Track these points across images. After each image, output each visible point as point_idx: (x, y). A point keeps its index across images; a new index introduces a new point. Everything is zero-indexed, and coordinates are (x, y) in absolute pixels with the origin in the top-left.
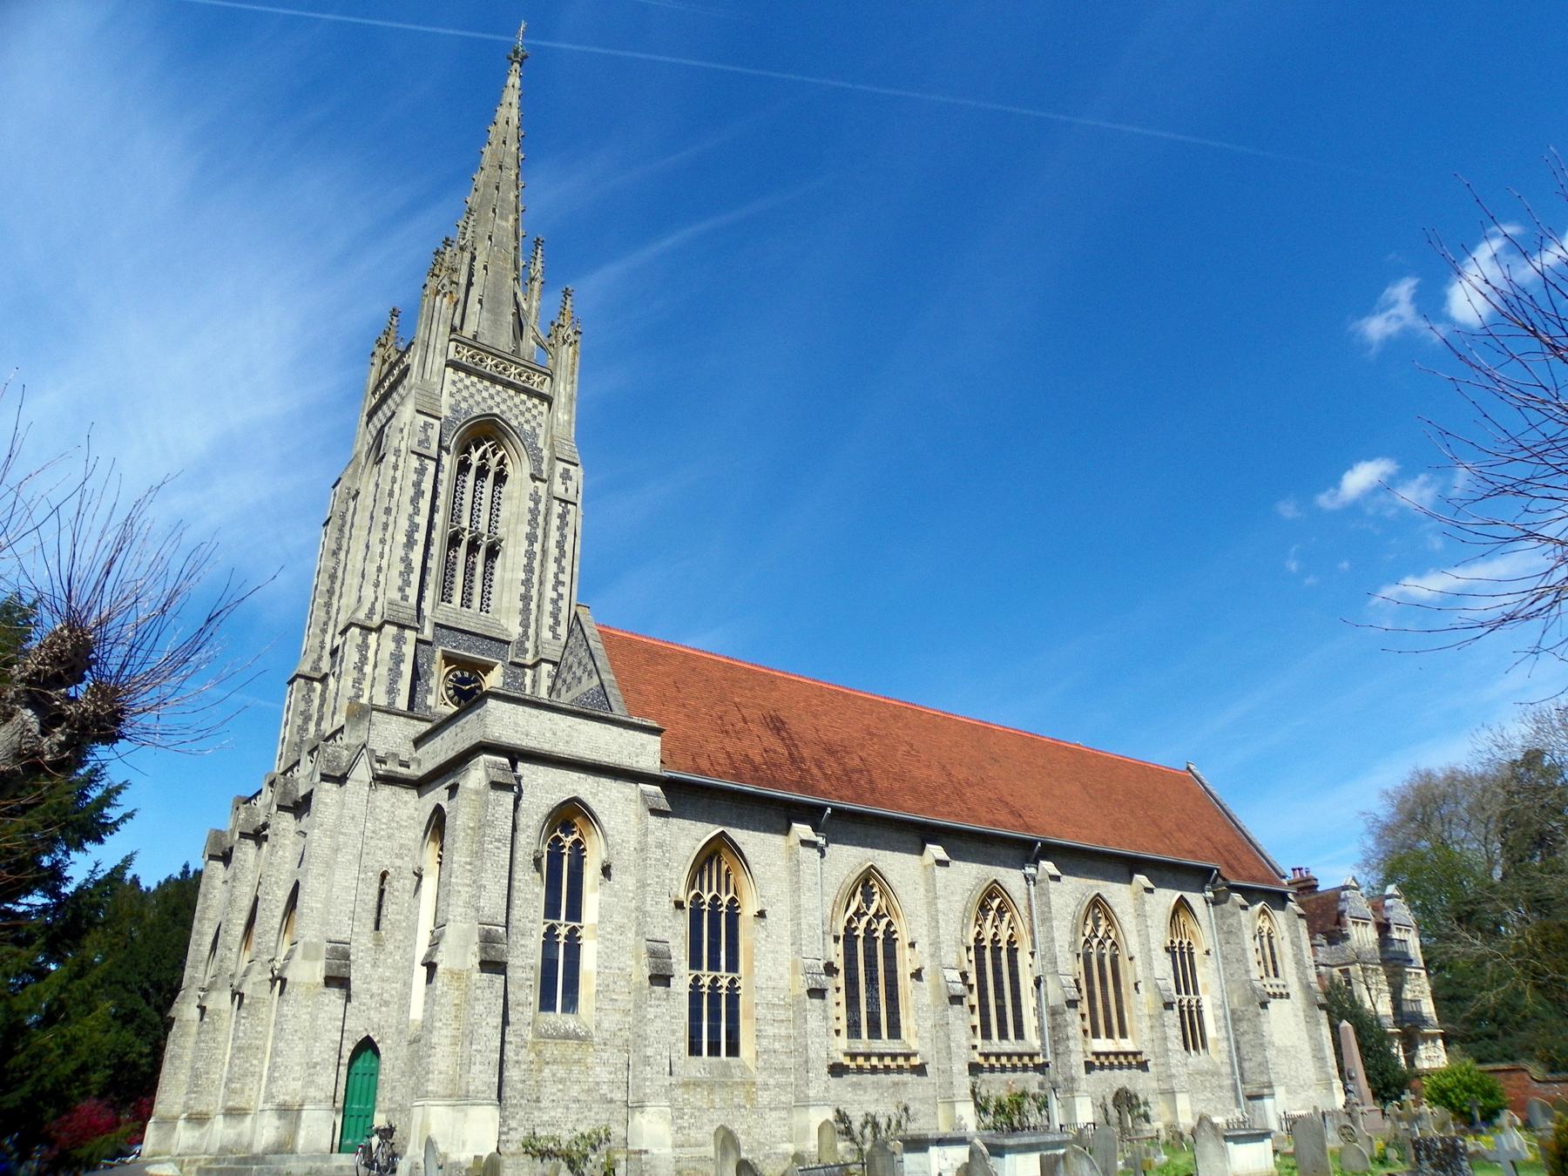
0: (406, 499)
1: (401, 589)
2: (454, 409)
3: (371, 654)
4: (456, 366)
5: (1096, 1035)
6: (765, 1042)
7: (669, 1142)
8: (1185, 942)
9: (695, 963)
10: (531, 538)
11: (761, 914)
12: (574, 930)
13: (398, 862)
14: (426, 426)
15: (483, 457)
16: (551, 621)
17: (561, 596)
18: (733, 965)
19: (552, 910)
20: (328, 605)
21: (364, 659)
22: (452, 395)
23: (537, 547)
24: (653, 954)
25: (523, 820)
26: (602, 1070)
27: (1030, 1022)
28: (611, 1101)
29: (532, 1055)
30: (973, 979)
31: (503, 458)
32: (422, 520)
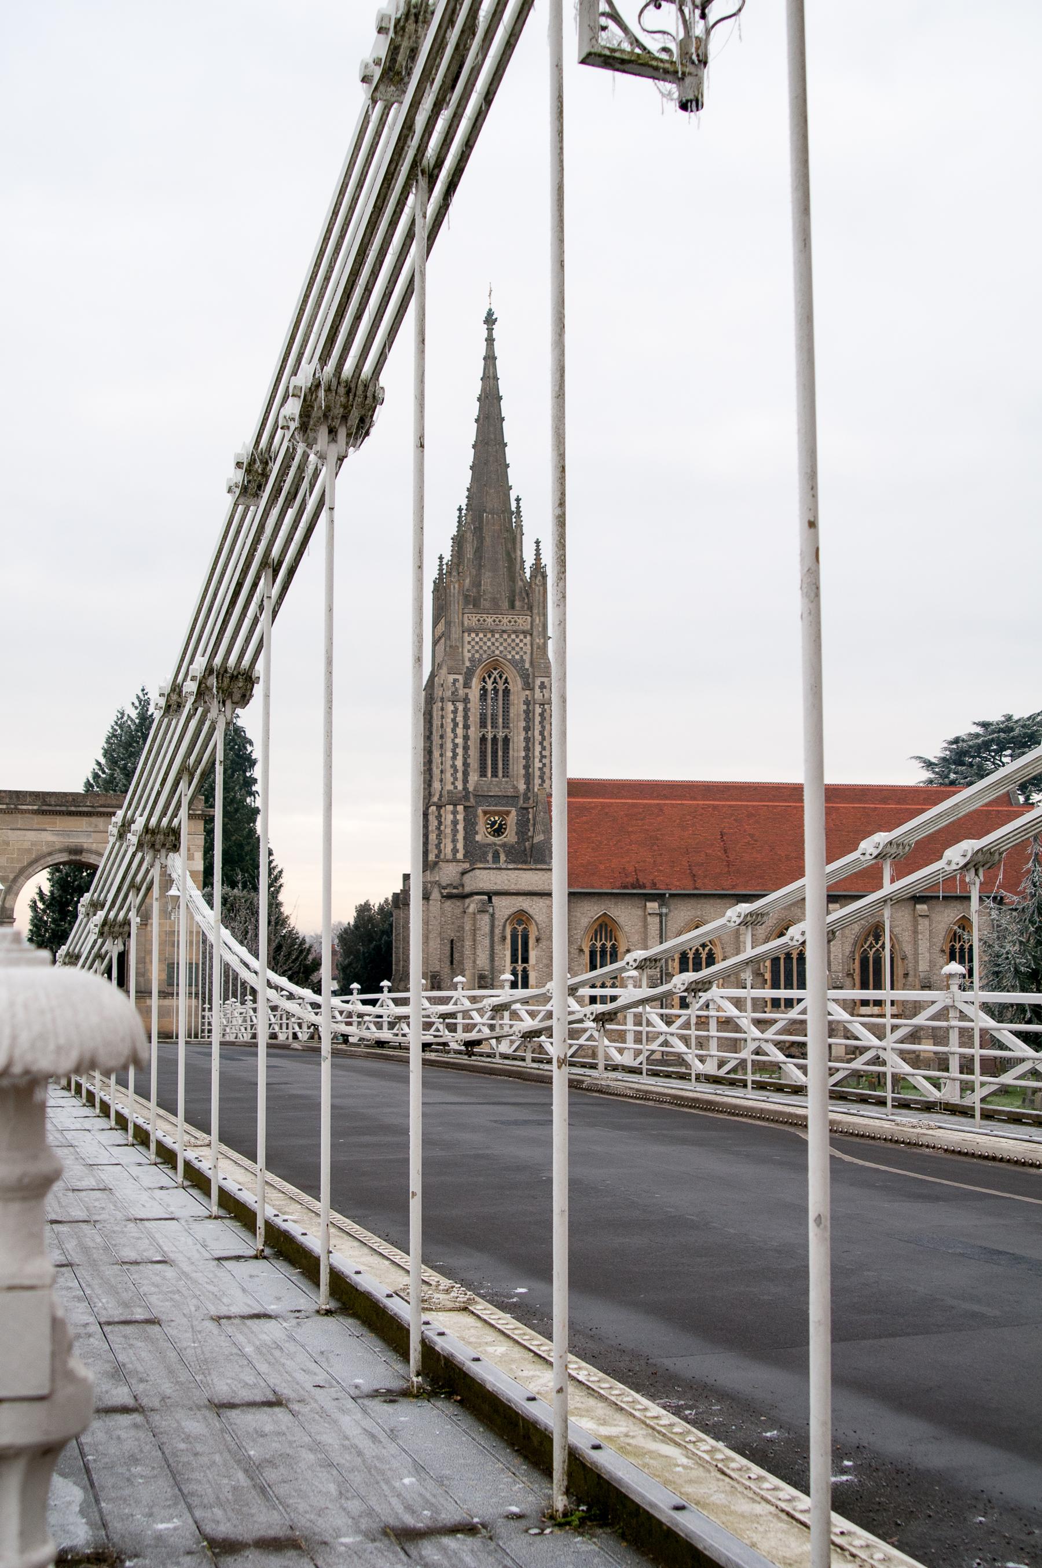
0: (449, 730)
1: (453, 783)
4: (470, 631)
10: (527, 729)
12: (525, 968)
14: (455, 680)
15: (495, 682)
17: (544, 765)
19: (514, 961)
21: (440, 823)
25: (496, 923)
31: (506, 679)
32: (459, 741)
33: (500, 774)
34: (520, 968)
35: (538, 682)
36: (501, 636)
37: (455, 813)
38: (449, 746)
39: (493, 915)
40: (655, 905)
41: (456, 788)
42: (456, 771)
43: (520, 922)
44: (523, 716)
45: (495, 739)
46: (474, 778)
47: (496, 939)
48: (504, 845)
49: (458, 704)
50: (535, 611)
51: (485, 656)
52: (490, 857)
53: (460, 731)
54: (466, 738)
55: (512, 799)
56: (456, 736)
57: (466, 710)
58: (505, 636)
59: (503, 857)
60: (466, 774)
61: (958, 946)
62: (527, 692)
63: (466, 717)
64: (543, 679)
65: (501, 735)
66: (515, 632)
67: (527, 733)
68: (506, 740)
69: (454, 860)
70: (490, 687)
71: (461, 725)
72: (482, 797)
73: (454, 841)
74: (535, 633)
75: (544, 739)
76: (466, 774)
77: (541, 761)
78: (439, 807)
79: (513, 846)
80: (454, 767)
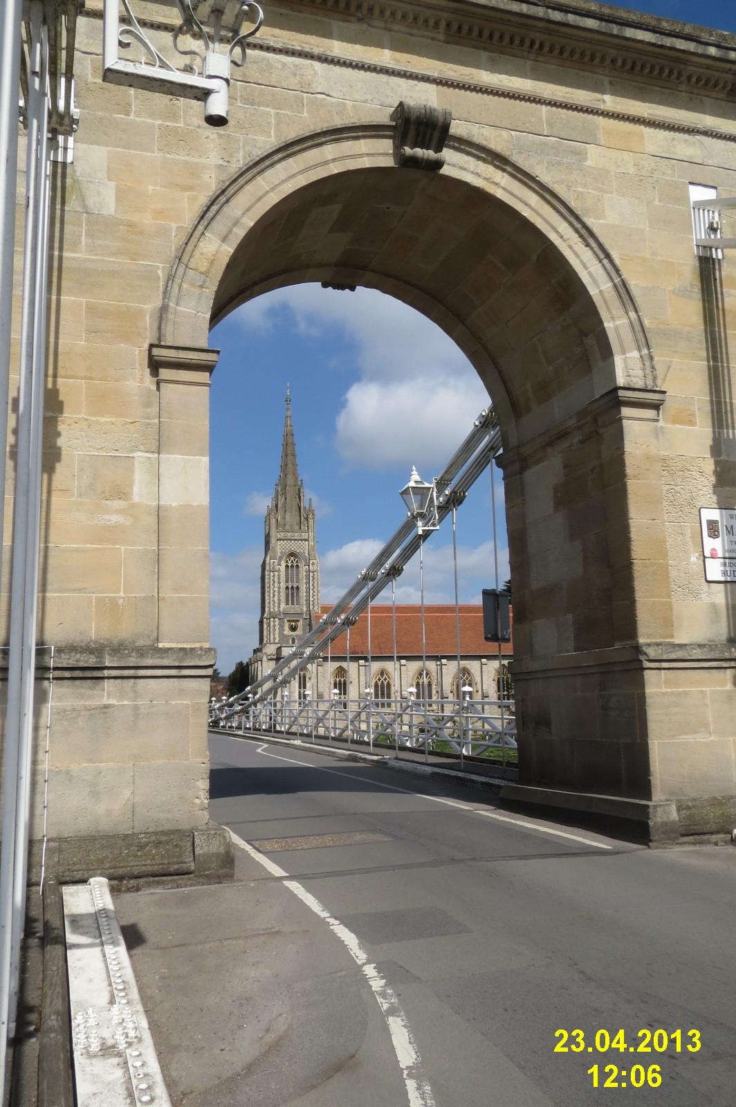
4: (280, 540)
14: (274, 562)
15: (292, 562)
17: (314, 599)
19: (300, 688)
34: (302, 691)
35: (311, 562)
37: (274, 622)
38: (272, 591)
40: (363, 661)
42: (274, 603)
45: (292, 588)
46: (283, 605)
49: (275, 573)
50: (310, 530)
52: (291, 642)
53: (276, 585)
54: (279, 588)
56: (274, 587)
57: (279, 575)
59: (296, 641)
60: (279, 604)
63: (279, 578)
65: (295, 586)
66: (300, 540)
68: (298, 588)
69: (274, 643)
70: (290, 565)
71: (276, 582)
73: (274, 634)
74: (310, 540)
75: (314, 587)
76: (279, 604)
80: (274, 601)
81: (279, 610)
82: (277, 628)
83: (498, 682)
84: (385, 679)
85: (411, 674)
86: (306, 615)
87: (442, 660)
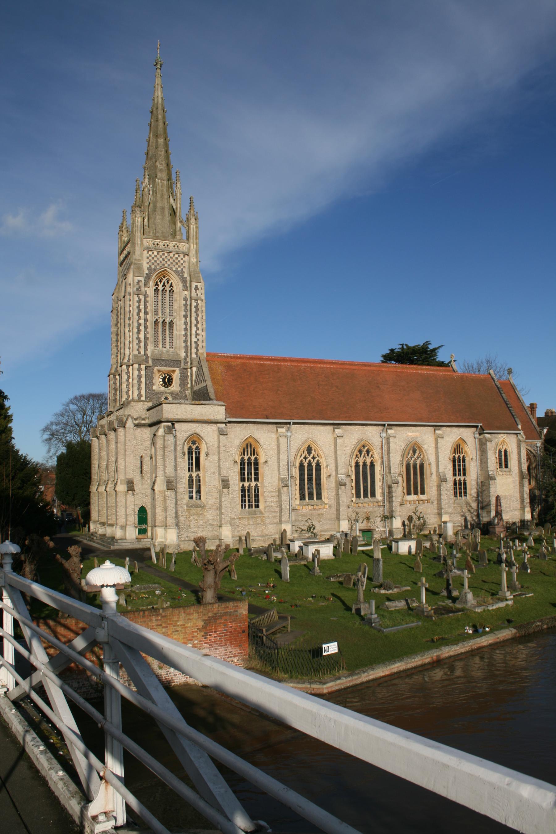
0: (135, 314)
1: (138, 350)
2: (149, 269)
3: (131, 375)
5: (409, 493)
6: (268, 503)
7: (231, 536)
8: (461, 456)
9: (243, 480)
10: (186, 317)
11: (266, 462)
13: (146, 452)
14: (139, 281)
15: (164, 285)
16: (195, 350)
17: (198, 340)
18: (257, 479)
19: (190, 469)
20: (117, 346)
21: (129, 377)
22: (147, 263)
23: (188, 320)
24: (223, 481)
25: (178, 443)
26: (210, 516)
27: (378, 491)
28: (213, 525)
29: (187, 513)
30: (353, 477)
31: (171, 284)
32: (142, 321)
33: (168, 345)
35: (194, 285)
36: (169, 255)
37: (139, 370)
39: (175, 437)
41: (140, 353)
42: (140, 341)
43: (194, 443)
44: (183, 308)
45: (164, 322)
47: (179, 454)
48: (171, 393)
49: (141, 296)
50: (191, 241)
51: (158, 267)
53: (142, 315)
54: (146, 320)
55: (175, 362)
56: (140, 318)
57: (146, 302)
58: (171, 255)
60: (146, 345)
61: (457, 456)
62: (186, 293)
63: (146, 307)
64: (197, 284)
65: (168, 321)
67: (186, 319)
68: (171, 324)
69: (139, 400)
70: (160, 288)
71: (143, 311)
72: (158, 361)
73: (139, 389)
74: (191, 254)
75: (198, 322)
76: (146, 345)
77: (196, 337)
78: (128, 366)
79: (177, 394)
80: (138, 338)
81: (145, 354)
82: (143, 380)
83: (454, 461)
84: (314, 458)
85: (349, 450)
86: (186, 363)
87: (389, 431)
